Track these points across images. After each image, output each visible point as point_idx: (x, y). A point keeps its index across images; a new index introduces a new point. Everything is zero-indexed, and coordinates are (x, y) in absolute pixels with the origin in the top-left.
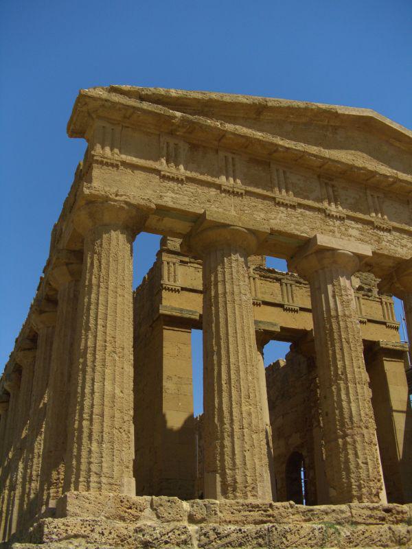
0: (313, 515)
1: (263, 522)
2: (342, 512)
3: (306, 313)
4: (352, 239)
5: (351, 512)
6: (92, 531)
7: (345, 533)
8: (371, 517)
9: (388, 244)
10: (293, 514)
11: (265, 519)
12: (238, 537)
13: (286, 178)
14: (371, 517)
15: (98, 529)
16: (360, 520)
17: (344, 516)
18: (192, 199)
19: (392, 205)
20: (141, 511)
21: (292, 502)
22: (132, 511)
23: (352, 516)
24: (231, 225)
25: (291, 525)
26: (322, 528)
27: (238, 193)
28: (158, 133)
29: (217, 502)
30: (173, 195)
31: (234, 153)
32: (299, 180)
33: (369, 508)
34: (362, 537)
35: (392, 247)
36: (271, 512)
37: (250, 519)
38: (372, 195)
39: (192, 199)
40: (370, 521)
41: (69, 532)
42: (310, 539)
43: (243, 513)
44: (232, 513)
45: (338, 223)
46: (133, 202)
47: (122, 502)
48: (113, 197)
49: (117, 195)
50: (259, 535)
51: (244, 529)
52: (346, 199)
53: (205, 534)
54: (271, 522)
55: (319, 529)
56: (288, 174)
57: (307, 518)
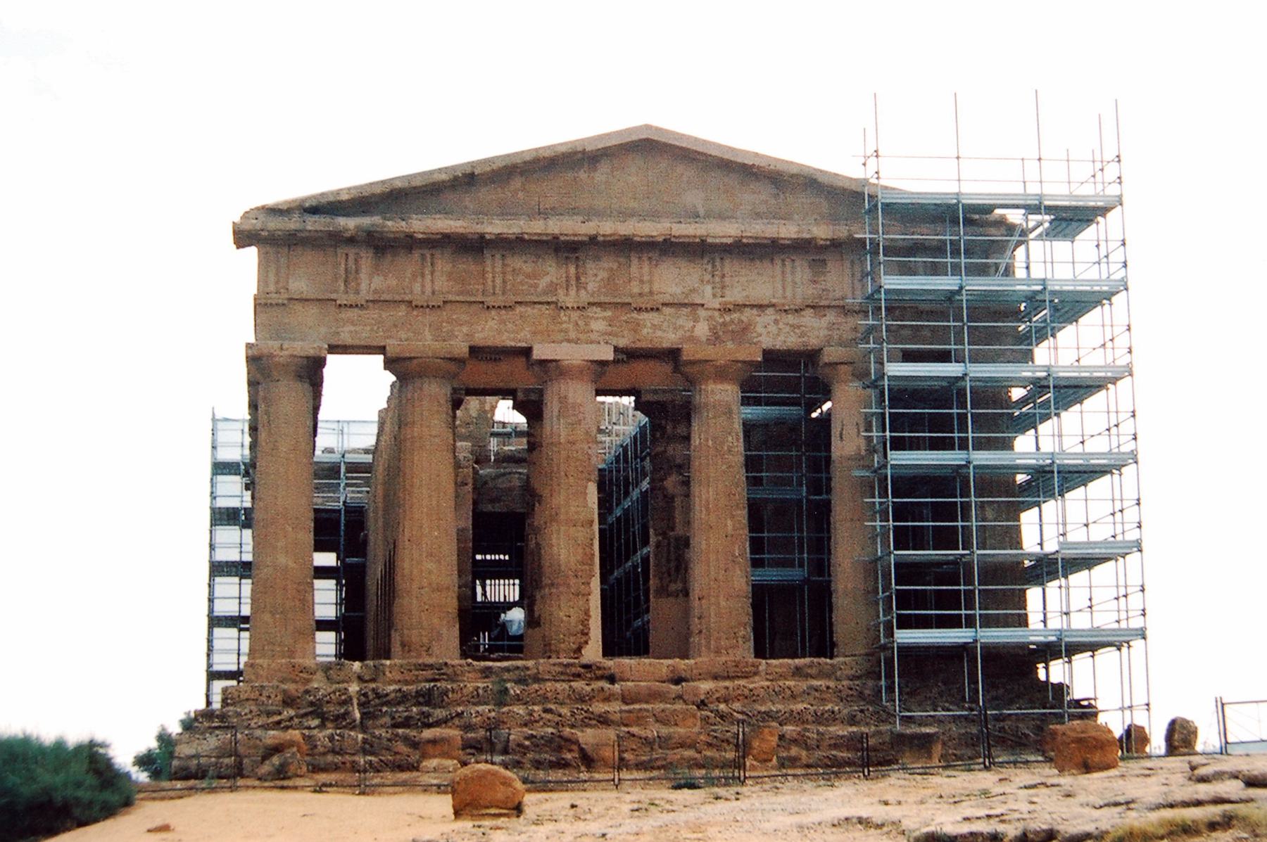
0: (491, 672)
2: (528, 669)
3: (652, 363)
5: (537, 669)
6: (261, 695)
7: (515, 691)
8: (562, 673)
10: (469, 672)
11: (437, 677)
12: (397, 697)
13: (504, 265)
14: (562, 673)
15: (265, 693)
17: (528, 673)
18: (375, 328)
20: (311, 674)
24: (414, 358)
26: (488, 687)
27: (433, 306)
28: (333, 243)
29: (388, 662)
30: (352, 328)
31: (433, 247)
32: (525, 262)
35: (659, 333)
38: (640, 258)
41: (241, 696)
42: (473, 697)
43: (417, 673)
44: (402, 673)
45: (575, 315)
48: (278, 352)
51: (405, 688)
52: (596, 275)
55: (484, 688)
57: (484, 675)
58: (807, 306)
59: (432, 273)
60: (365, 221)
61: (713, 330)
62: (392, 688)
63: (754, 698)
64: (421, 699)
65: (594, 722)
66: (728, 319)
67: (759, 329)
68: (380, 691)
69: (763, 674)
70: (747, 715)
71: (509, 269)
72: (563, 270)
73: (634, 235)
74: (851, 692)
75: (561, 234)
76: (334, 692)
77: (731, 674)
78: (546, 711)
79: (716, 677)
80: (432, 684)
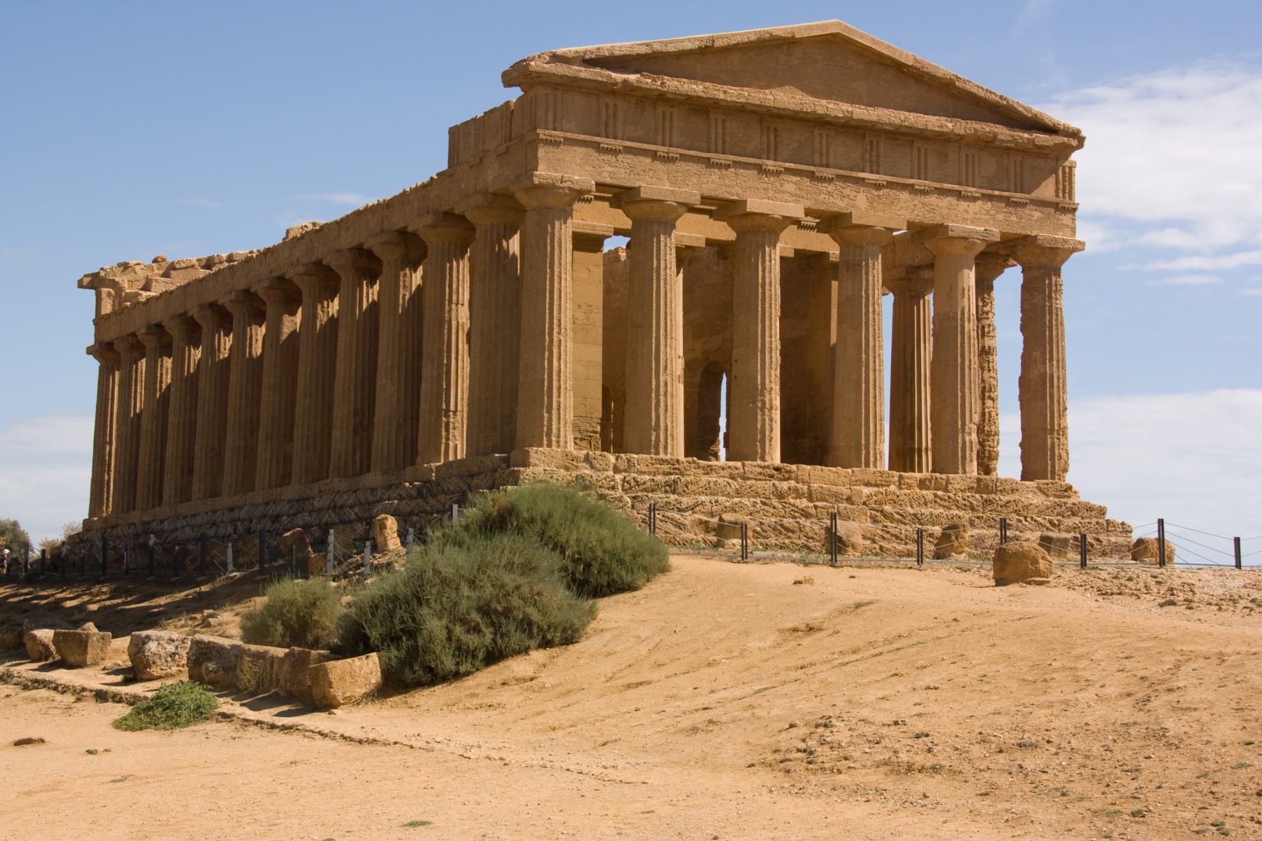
0: (711, 470)
1: (670, 474)
2: (737, 468)
4: (787, 196)
8: (761, 474)
9: (826, 197)
13: (724, 128)
15: (555, 476)
16: (750, 476)
17: (737, 471)
18: (628, 171)
19: (843, 142)
21: (695, 459)
22: (575, 463)
23: (745, 473)
25: (692, 477)
29: (636, 456)
30: (611, 169)
31: (672, 106)
33: (761, 467)
34: (749, 490)
36: (677, 466)
37: (661, 471)
39: (628, 171)
40: (760, 477)
46: (577, 187)
47: (567, 455)
48: (558, 184)
49: (562, 182)
50: (667, 484)
52: (789, 145)
53: (627, 482)
54: (677, 474)
56: (728, 124)
58: (935, 188)
59: (671, 128)
60: (633, 77)
61: (871, 202)
62: (648, 478)
63: (900, 502)
64: (668, 488)
65: (796, 514)
66: (881, 193)
67: (901, 204)
68: (639, 479)
69: (897, 483)
70: (902, 515)
71: (728, 132)
72: (765, 138)
73: (826, 115)
74: (965, 502)
75: (774, 108)
76: (605, 479)
77: (878, 482)
78: (764, 504)
79: (867, 484)
80: (677, 476)
